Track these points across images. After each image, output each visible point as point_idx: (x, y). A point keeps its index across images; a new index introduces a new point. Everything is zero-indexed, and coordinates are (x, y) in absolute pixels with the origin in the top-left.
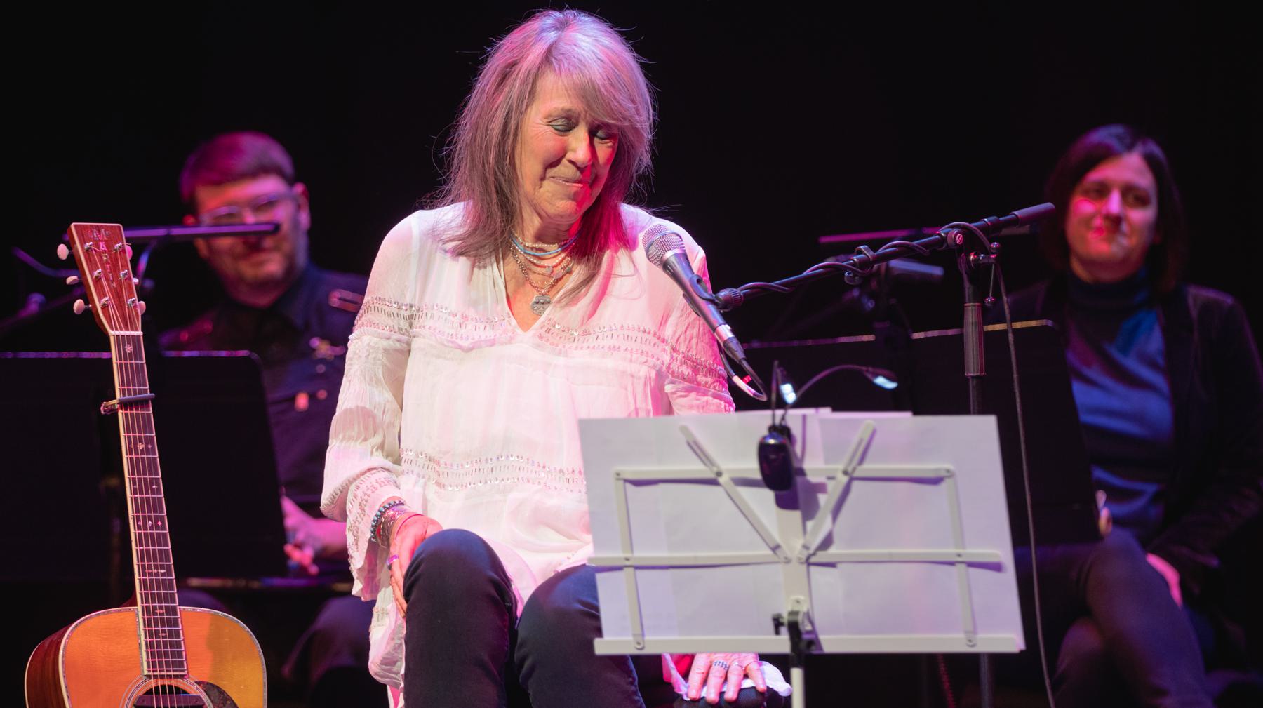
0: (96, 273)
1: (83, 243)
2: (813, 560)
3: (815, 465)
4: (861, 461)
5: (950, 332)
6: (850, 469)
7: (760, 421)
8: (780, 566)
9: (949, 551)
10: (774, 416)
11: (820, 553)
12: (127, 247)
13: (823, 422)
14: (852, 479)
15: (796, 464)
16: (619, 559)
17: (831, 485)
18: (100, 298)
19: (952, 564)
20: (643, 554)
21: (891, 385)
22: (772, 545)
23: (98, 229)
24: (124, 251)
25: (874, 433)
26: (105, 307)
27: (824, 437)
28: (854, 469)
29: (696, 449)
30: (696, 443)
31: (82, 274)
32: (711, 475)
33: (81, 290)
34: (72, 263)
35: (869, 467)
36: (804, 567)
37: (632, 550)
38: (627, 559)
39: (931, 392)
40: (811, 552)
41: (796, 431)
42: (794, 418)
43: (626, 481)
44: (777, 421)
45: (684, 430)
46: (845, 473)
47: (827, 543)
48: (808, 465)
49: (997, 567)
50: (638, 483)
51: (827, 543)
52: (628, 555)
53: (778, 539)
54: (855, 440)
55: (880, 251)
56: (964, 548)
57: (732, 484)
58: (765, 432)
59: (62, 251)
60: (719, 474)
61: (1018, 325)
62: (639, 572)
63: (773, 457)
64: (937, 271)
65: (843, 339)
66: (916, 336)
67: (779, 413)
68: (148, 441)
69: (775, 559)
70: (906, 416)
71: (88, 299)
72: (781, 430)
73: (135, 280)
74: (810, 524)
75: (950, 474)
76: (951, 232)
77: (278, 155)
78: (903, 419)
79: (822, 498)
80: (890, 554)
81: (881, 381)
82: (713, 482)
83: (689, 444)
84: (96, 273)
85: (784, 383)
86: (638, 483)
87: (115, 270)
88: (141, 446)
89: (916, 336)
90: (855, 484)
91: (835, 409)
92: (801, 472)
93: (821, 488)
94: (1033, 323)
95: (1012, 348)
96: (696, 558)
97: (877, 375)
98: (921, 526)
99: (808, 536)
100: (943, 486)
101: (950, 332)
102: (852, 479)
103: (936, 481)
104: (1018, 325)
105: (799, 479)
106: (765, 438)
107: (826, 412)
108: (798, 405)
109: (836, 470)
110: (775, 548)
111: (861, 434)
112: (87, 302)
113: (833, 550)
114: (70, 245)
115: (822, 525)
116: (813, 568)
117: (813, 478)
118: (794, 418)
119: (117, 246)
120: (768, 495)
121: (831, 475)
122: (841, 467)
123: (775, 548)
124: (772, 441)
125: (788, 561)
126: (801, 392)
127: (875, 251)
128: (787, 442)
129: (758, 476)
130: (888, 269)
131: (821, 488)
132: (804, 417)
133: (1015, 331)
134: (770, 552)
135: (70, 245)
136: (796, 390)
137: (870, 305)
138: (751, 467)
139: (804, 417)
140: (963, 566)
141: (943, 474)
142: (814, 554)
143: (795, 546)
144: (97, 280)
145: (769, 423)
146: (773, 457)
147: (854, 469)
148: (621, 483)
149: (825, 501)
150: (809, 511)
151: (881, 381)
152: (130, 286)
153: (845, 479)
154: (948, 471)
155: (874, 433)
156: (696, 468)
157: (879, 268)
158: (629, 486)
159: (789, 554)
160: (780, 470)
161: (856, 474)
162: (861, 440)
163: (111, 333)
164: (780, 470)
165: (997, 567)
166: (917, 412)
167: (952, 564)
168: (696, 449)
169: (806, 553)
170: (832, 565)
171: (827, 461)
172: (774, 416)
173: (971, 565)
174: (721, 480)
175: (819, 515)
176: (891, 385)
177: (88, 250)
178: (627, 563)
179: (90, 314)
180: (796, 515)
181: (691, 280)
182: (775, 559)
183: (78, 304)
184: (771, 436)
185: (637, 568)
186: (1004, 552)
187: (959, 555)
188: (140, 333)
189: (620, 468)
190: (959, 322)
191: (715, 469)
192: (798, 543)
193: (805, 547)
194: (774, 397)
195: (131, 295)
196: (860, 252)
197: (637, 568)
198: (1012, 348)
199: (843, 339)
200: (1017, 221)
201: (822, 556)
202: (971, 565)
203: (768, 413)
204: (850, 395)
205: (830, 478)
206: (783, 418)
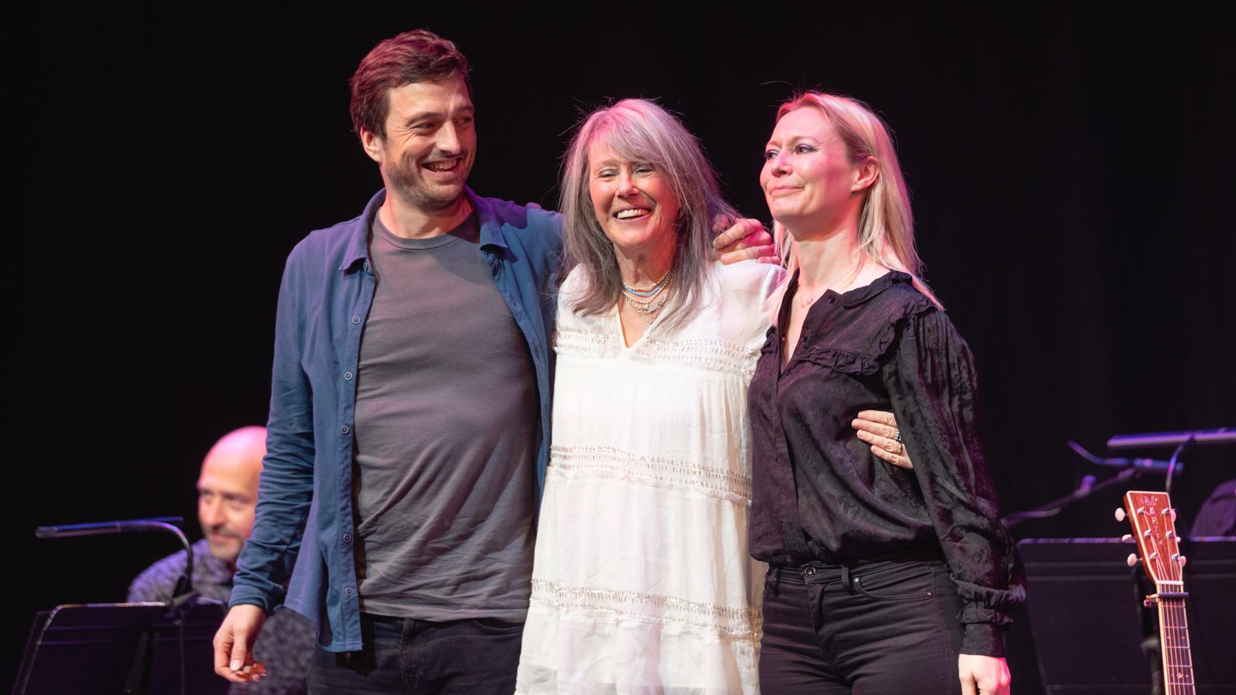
0: (1147, 533)
1: (1136, 507)
12: (1173, 512)
18: (1149, 553)
23: (1149, 496)
24: (1168, 514)
26: (1153, 561)
31: (1134, 533)
33: (1135, 548)
34: (1127, 525)
59: (1120, 514)
68: (1186, 671)
71: (1139, 554)
73: (1178, 539)
84: (1147, 533)
87: (1163, 530)
88: (1180, 676)
112: (1138, 557)
114: (1126, 510)
119: (1164, 511)
135: (1126, 510)
144: (1147, 539)
152: (1173, 543)
163: (1158, 582)
177: (1142, 514)
179: (1141, 568)
183: (1132, 559)
188: (1181, 583)
195: (1174, 552)
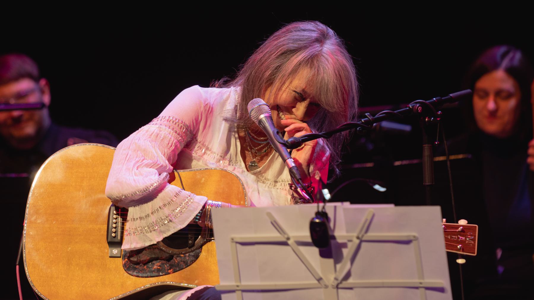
2: (340, 286)
3: (340, 233)
4: (367, 231)
5: (415, 161)
6: (360, 236)
7: (312, 209)
8: (322, 290)
9: (415, 281)
10: (318, 207)
11: (344, 282)
13: (345, 210)
14: (361, 241)
15: (330, 233)
16: (233, 286)
17: (350, 245)
19: (417, 288)
20: (246, 283)
21: (382, 189)
22: (317, 278)
25: (373, 216)
27: (347, 218)
28: (363, 236)
29: (275, 225)
30: (275, 222)
32: (283, 239)
35: (371, 235)
36: (335, 290)
37: (240, 281)
38: (238, 286)
39: (403, 194)
40: (339, 282)
41: (331, 215)
42: (329, 208)
43: (237, 243)
44: (320, 209)
45: (269, 215)
46: (358, 238)
47: (348, 276)
48: (337, 234)
49: (441, 290)
50: (243, 244)
51: (348, 276)
52: (238, 284)
53: (321, 275)
54: (363, 220)
55: (376, 116)
56: (423, 278)
57: (295, 245)
58: (313, 216)
60: (288, 239)
61: (452, 157)
62: (245, 294)
63: (318, 229)
64: (407, 128)
65: (356, 166)
66: (397, 163)
67: (321, 205)
69: (319, 285)
70: (391, 206)
72: (322, 215)
74: (338, 266)
75: (416, 238)
76: (415, 105)
77: (29, 66)
78: (390, 208)
79: (345, 251)
80: (383, 283)
81: (377, 187)
82: (285, 244)
83: (272, 223)
85: (324, 188)
86: (243, 244)
89: (397, 163)
90: (364, 245)
91: (352, 203)
92: (334, 238)
93: (344, 245)
94: (461, 156)
95: (449, 169)
96: (276, 285)
97: (375, 185)
98: (400, 268)
99: (337, 273)
100: (412, 245)
101: (415, 161)
102: (361, 241)
103: (407, 242)
104: (452, 157)
105: (332, 242)
106: (313, 219)
107: (347, 204)
108: (330, 201)
109: (353, 236)
110: (319, 280)
111: (366, 216)
113: (351, 281)
115: (344, 266)
116: (340, 291)
117: (340, 241)
118: (329, 208)
120: (315, 250)
121: (350, 239)
122: (355, 234)
123: (319, 280)
124: (317, 221)
125: (326, 287)
126: (333, 193)
127: (374, 115)
128: (326, 221)
129: (309, 240)
130: (381, 127)
131: (344, 245)
132: (335, 207)
133: (451, 161)
134: (316, 282)
136: (330, 192)
137: (370, 147)
138: (306, 234)
139: (335, 207)
140: (423, 289)
141: (412, 238)
142: (341, 283)
143: (330, 278)
145: (316, 210)
146: (318, 229)
147: (363, 236)
148: (234, 244)
149: (347, 252)
150: (338, 259)
151: (377, 187)
153: (357, 241)
154: (414, 237)
155: (373, 216)
156: (275, 235)
157: (376, 126)
158: (238, 245)
159: (327, 283)
160: (322, 236)
161: (364, 239)
162: (366, 220)
164: (322, 236)
165: (441, 290)
166: (397, 204)
167: (417, 288)
168: (275, 225)
169: (336, 282)
170: (351, 288)
171: (347, 231)
172: (318, 207)
173: (427, 288)
174: (290, 242)
175: (344, 261)
176: (382, 189)
178: (238, 288)
180: (331, 261)
181: (273, 132)
182: (319, 285)
184: (317, 218)
185: (243, 291)
186: (445, 281)
187: (421, 283)
189: (233, 236)
190: (420, 155)
191: (286, 236)
192: (332, 277)
193: (336, 279)
194: (318, 196)
196: (366, 117)
197: (243, 291)
198: (449, 169)
199: (356, 166)
200: (452, 99)
201: (345, 284)
202: (427, 288)
203: (315, 205)
204: (360, 194)
205: (350, 241)
206: (324, 208)
